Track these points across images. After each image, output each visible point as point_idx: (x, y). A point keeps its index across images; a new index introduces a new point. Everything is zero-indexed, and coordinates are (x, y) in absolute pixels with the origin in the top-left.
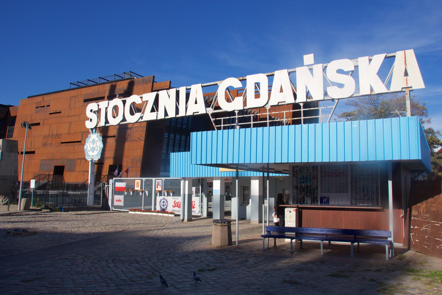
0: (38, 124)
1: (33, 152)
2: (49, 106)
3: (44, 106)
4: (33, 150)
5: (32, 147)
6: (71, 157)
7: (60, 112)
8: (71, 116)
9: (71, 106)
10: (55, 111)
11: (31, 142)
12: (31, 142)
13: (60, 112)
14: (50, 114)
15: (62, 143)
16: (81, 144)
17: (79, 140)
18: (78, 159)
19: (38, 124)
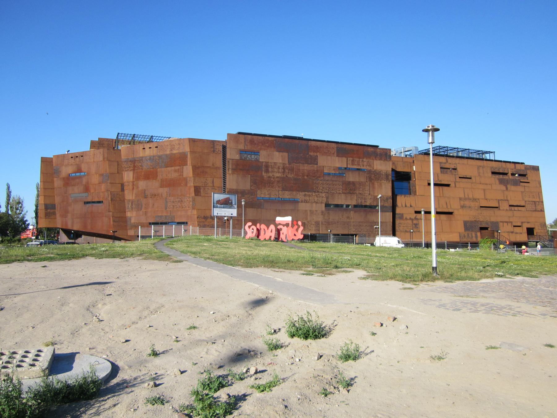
0: (448, 185)
1: (451, 213)
2: (456, 169)
3: (449, 169)
4: (451, 211)
5: (449, 207)
6: (493, 219)
7: (470, 178)
8: (483, 184)
9: (480, 174)
10: (465, 176)
11: (446, 203)
12: (446, 203)
13: (470, 178)
14: (460, 177)
15: (481, 207)
16: (500, 209)
17: (497, 206)
18: (501, 222)
19: (448, 185)
